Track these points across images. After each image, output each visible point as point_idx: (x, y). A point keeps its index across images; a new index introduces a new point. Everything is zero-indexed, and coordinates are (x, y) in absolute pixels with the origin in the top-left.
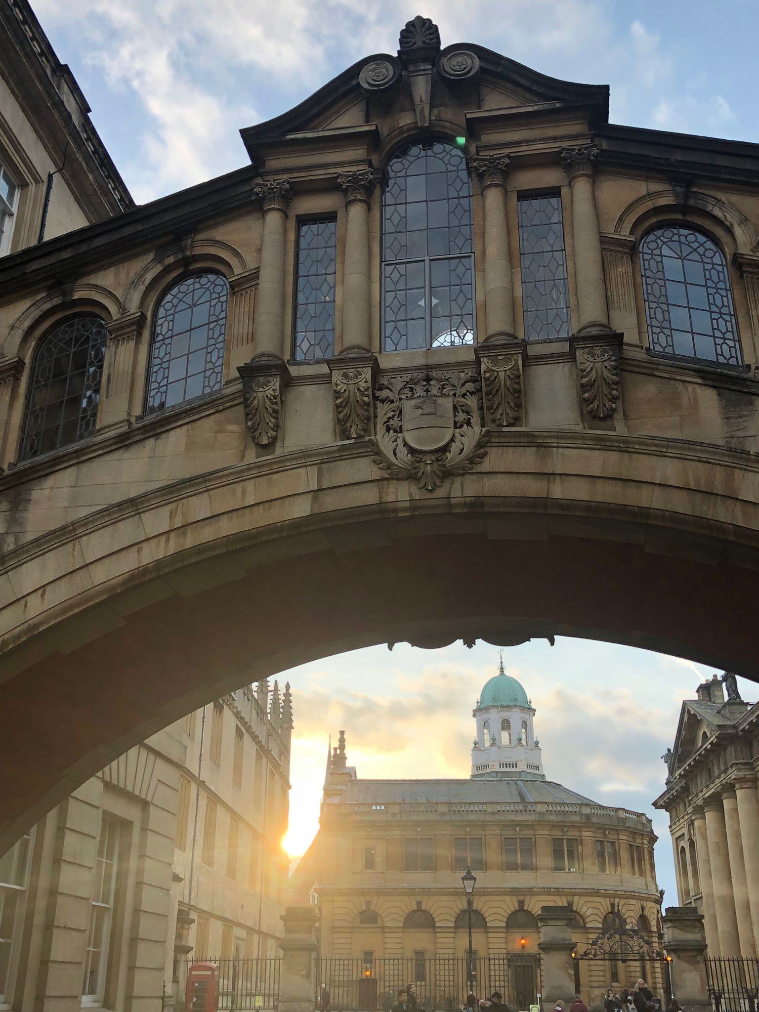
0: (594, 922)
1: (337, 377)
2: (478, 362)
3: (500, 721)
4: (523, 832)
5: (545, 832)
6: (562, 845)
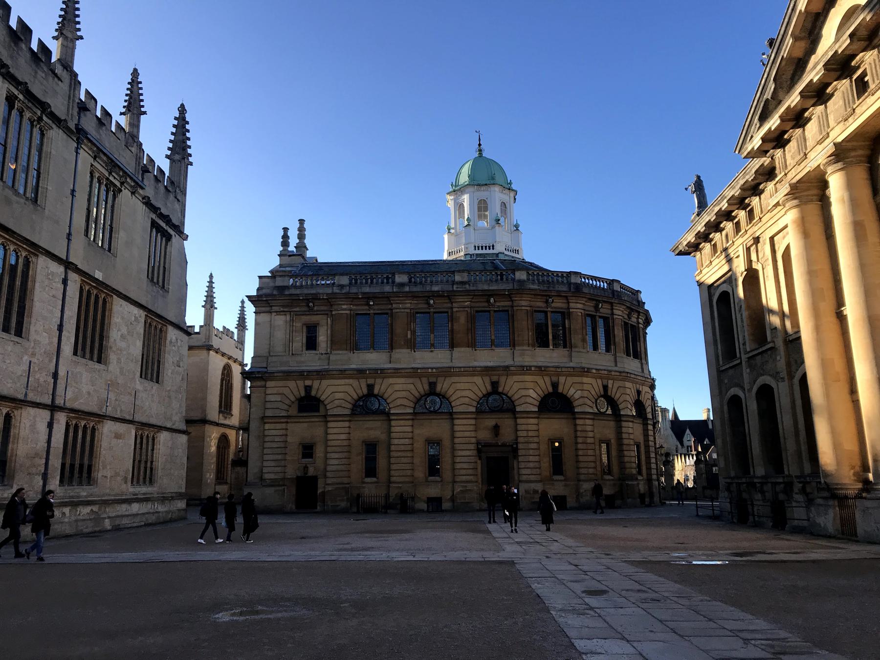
3: (476, 202)
4: (498, 304)
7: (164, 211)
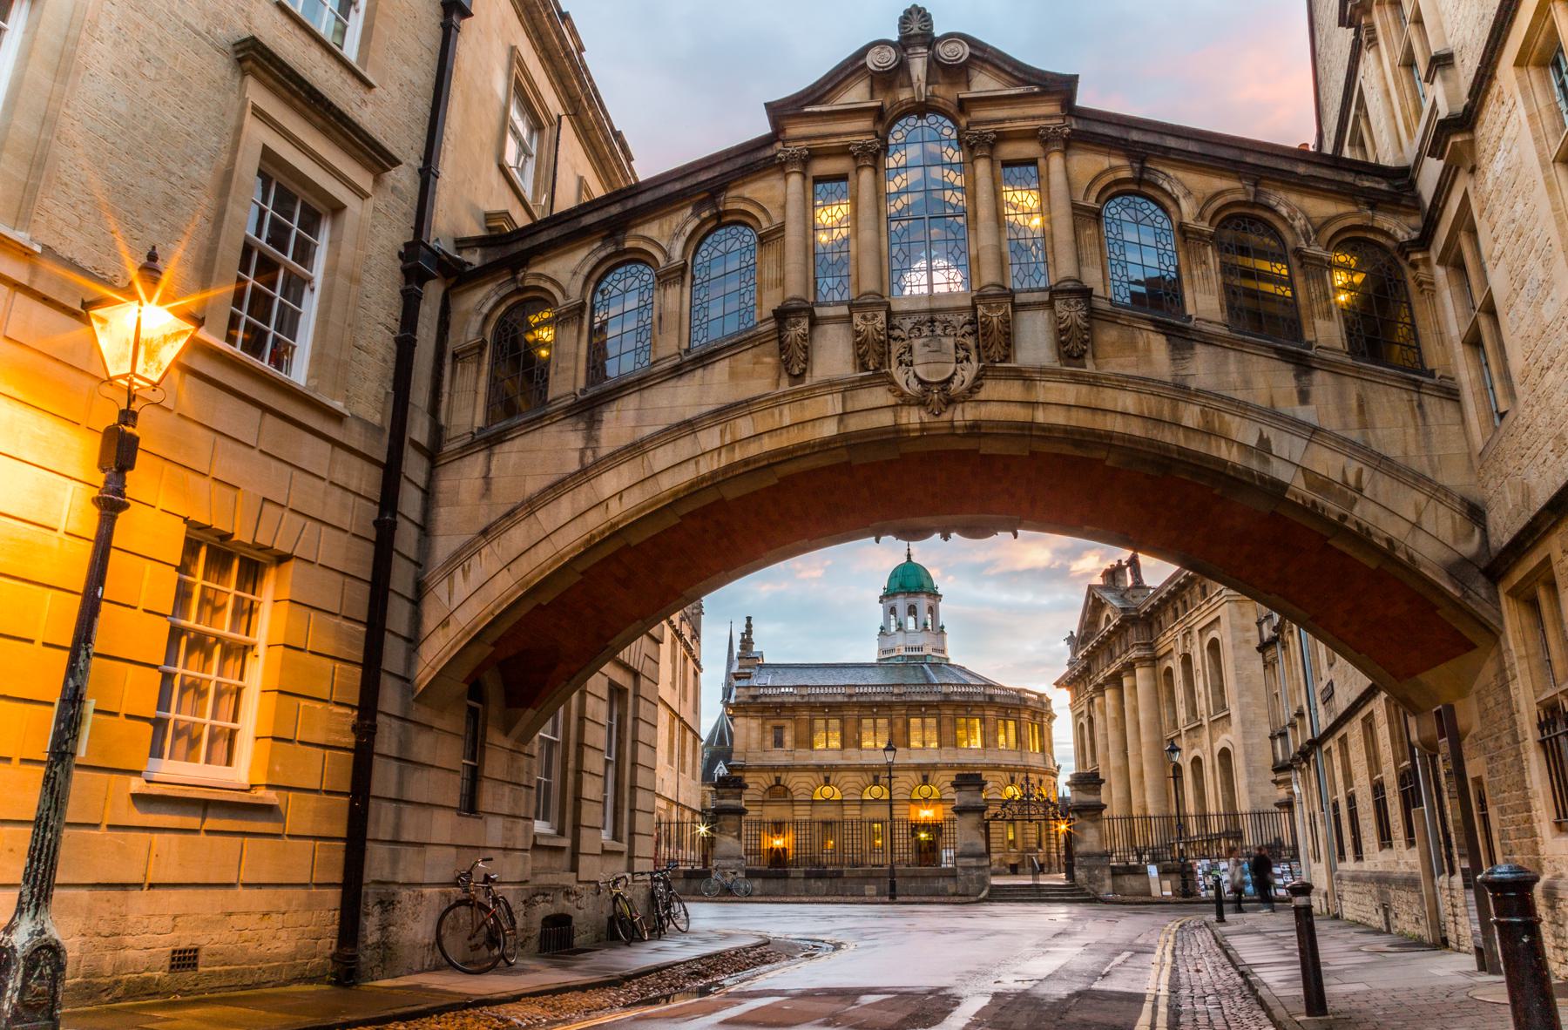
1: (857, 318)
2: (974, 308)
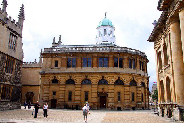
0: (127, 83)
5: (112, 55)
6: (118, 59)
7: (14, 30)
